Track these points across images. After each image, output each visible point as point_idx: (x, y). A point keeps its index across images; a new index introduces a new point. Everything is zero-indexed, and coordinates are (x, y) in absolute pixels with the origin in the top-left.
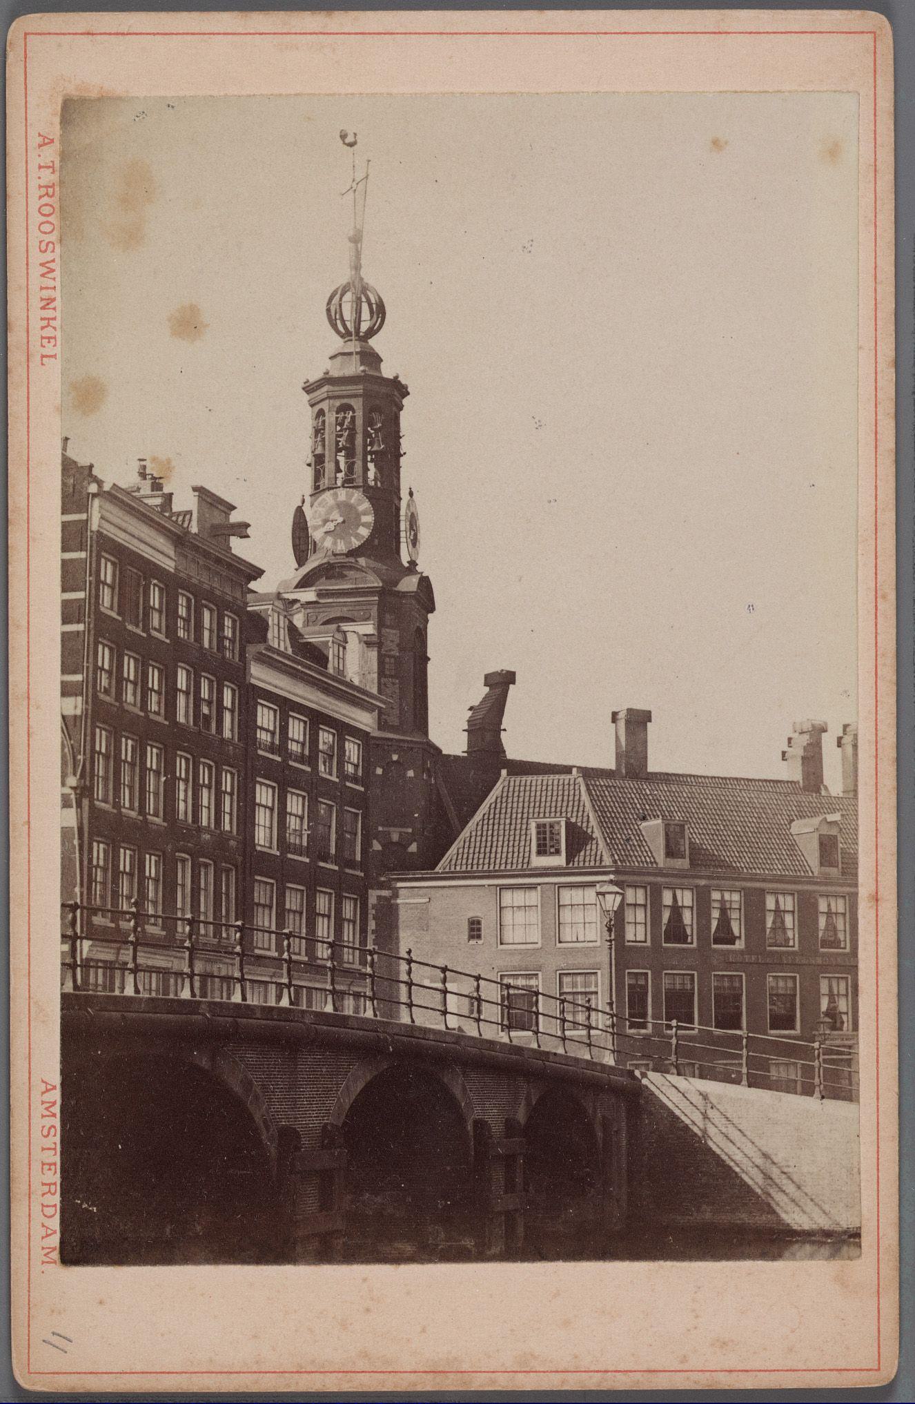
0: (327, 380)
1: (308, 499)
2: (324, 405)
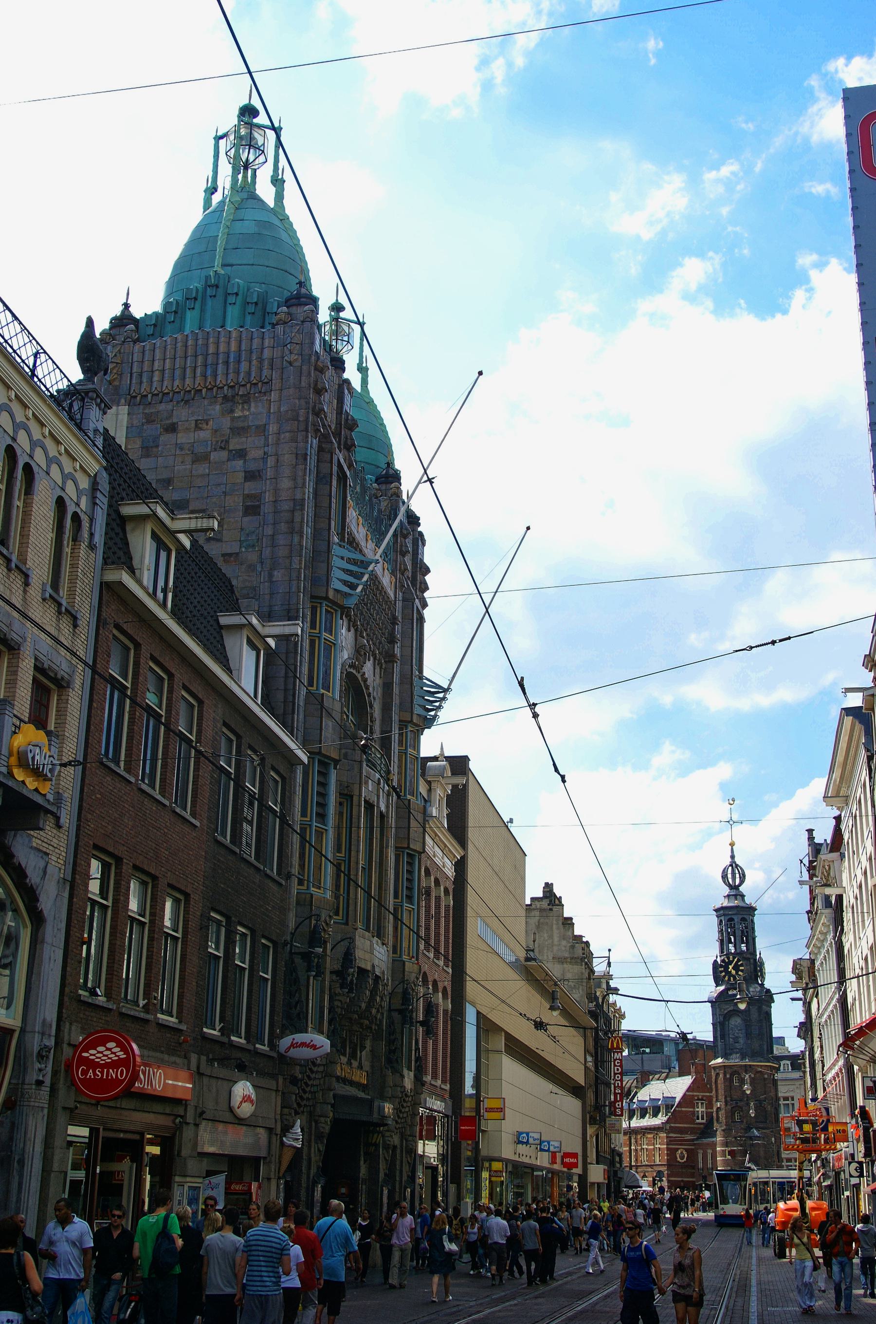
0: (722, 908)
2: (722, 918)
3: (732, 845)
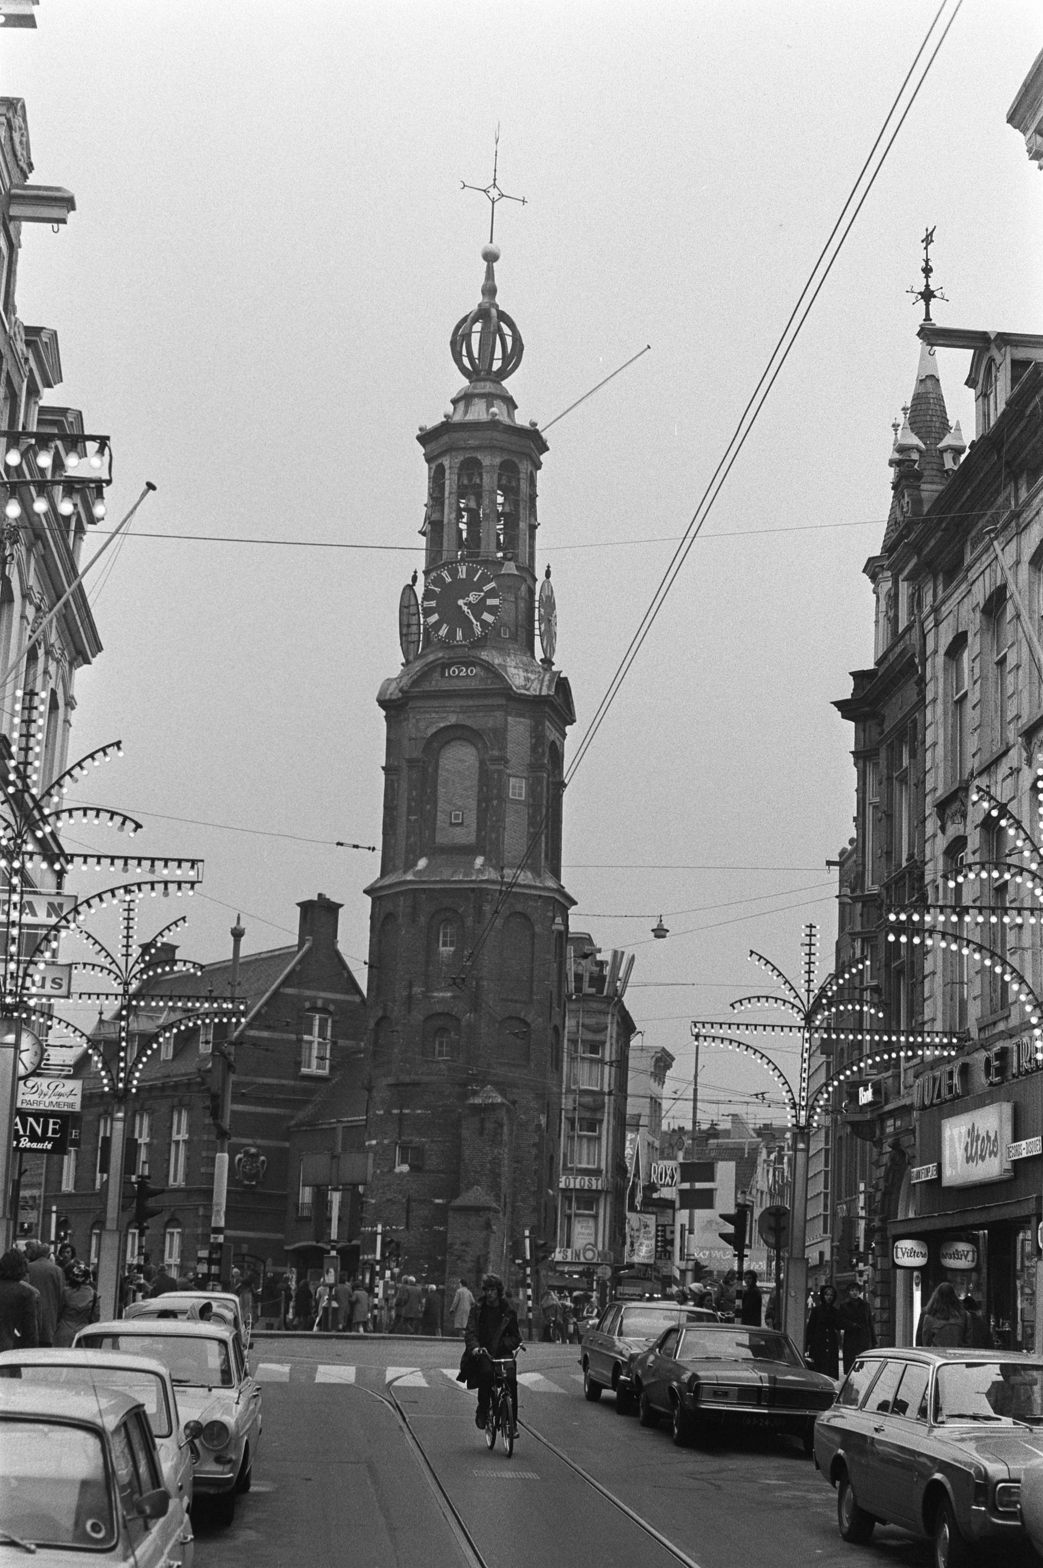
0: (446, 427)
1: (421, 578)
3: (490, 258)
